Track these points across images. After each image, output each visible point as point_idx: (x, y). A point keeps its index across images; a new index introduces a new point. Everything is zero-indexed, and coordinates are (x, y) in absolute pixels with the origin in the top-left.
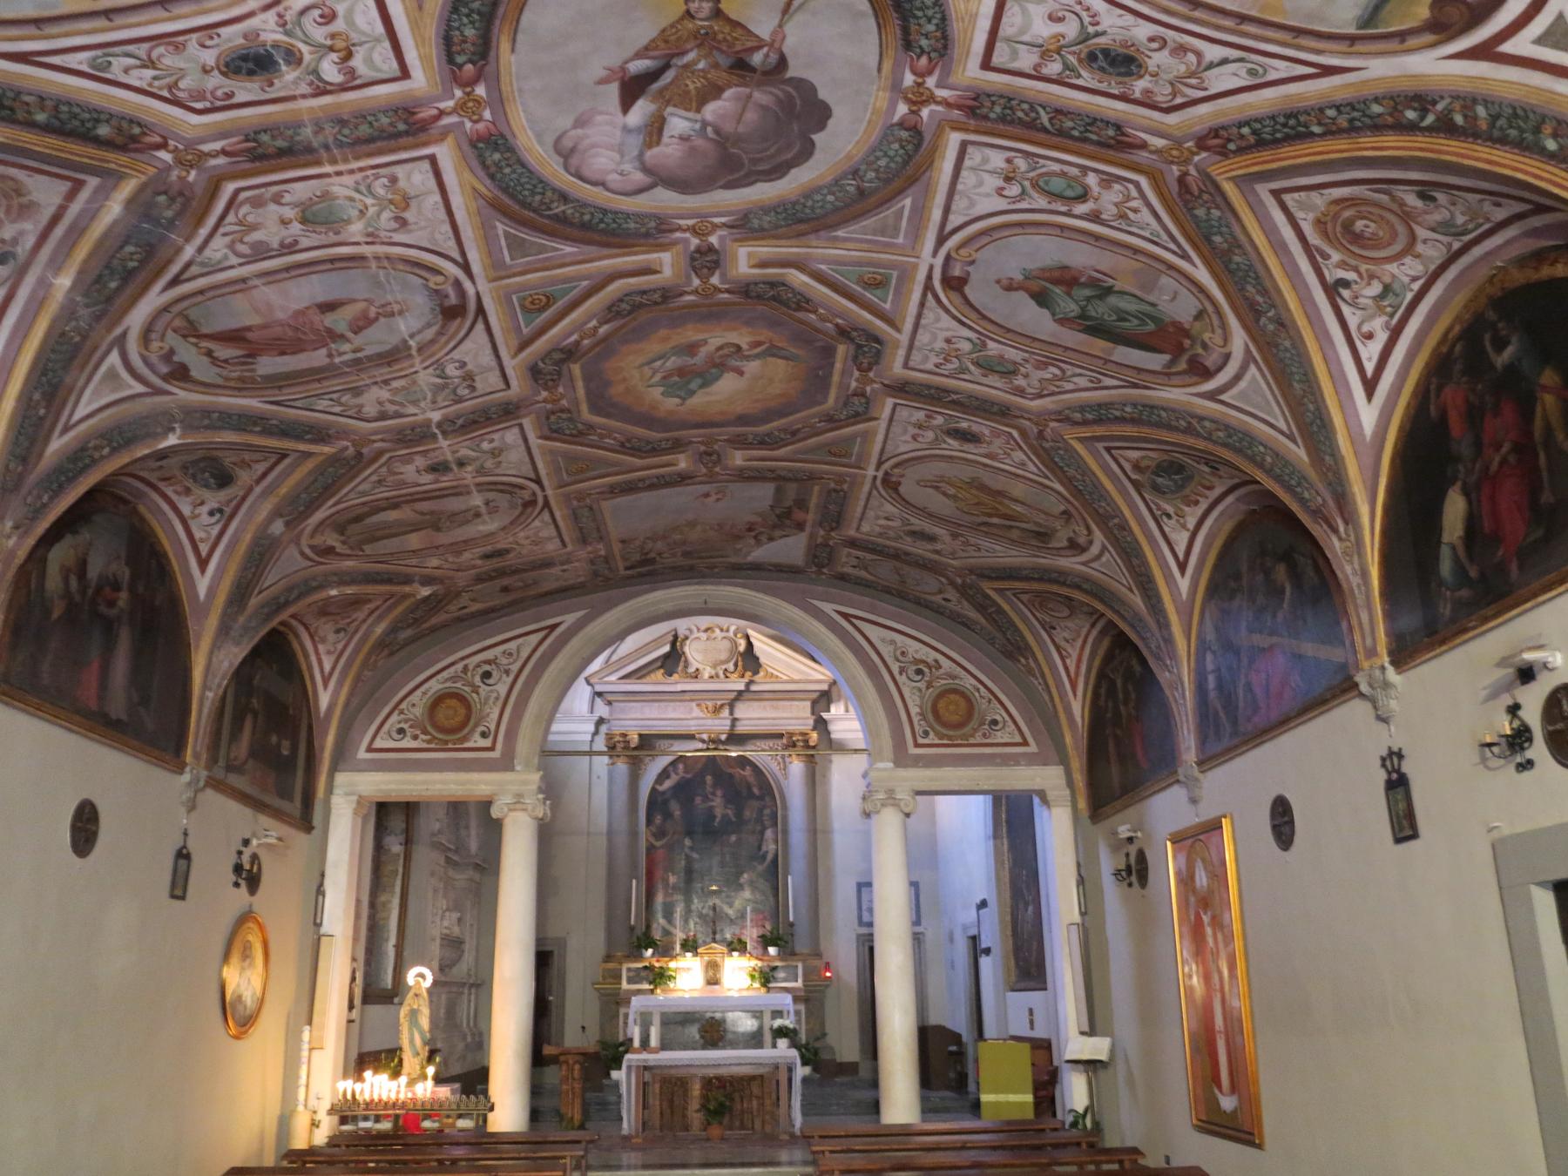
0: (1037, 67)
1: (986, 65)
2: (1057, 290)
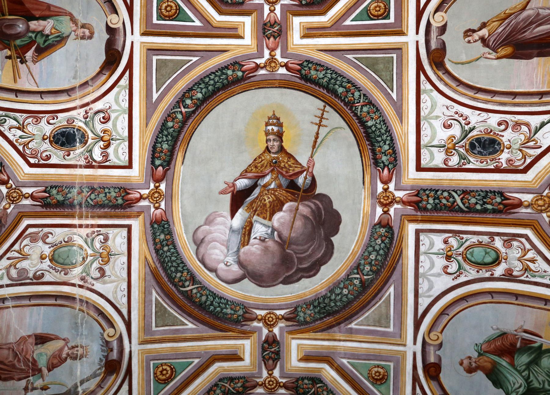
0: (445, 162)
1: (419, 168)
2: (504, 362)
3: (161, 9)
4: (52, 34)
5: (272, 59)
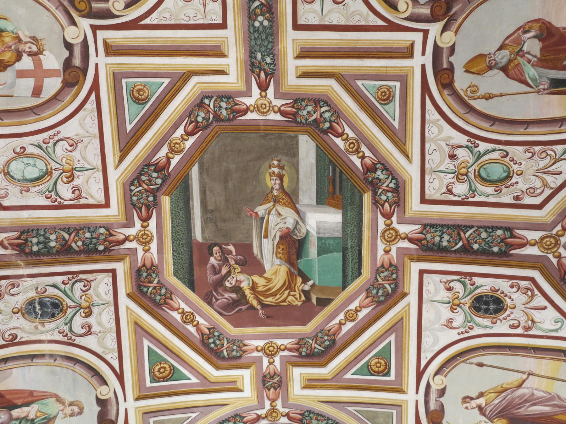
3: (154, 372)
4: (37, 417)
5: (273, 409)
